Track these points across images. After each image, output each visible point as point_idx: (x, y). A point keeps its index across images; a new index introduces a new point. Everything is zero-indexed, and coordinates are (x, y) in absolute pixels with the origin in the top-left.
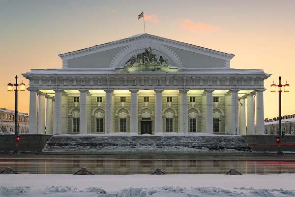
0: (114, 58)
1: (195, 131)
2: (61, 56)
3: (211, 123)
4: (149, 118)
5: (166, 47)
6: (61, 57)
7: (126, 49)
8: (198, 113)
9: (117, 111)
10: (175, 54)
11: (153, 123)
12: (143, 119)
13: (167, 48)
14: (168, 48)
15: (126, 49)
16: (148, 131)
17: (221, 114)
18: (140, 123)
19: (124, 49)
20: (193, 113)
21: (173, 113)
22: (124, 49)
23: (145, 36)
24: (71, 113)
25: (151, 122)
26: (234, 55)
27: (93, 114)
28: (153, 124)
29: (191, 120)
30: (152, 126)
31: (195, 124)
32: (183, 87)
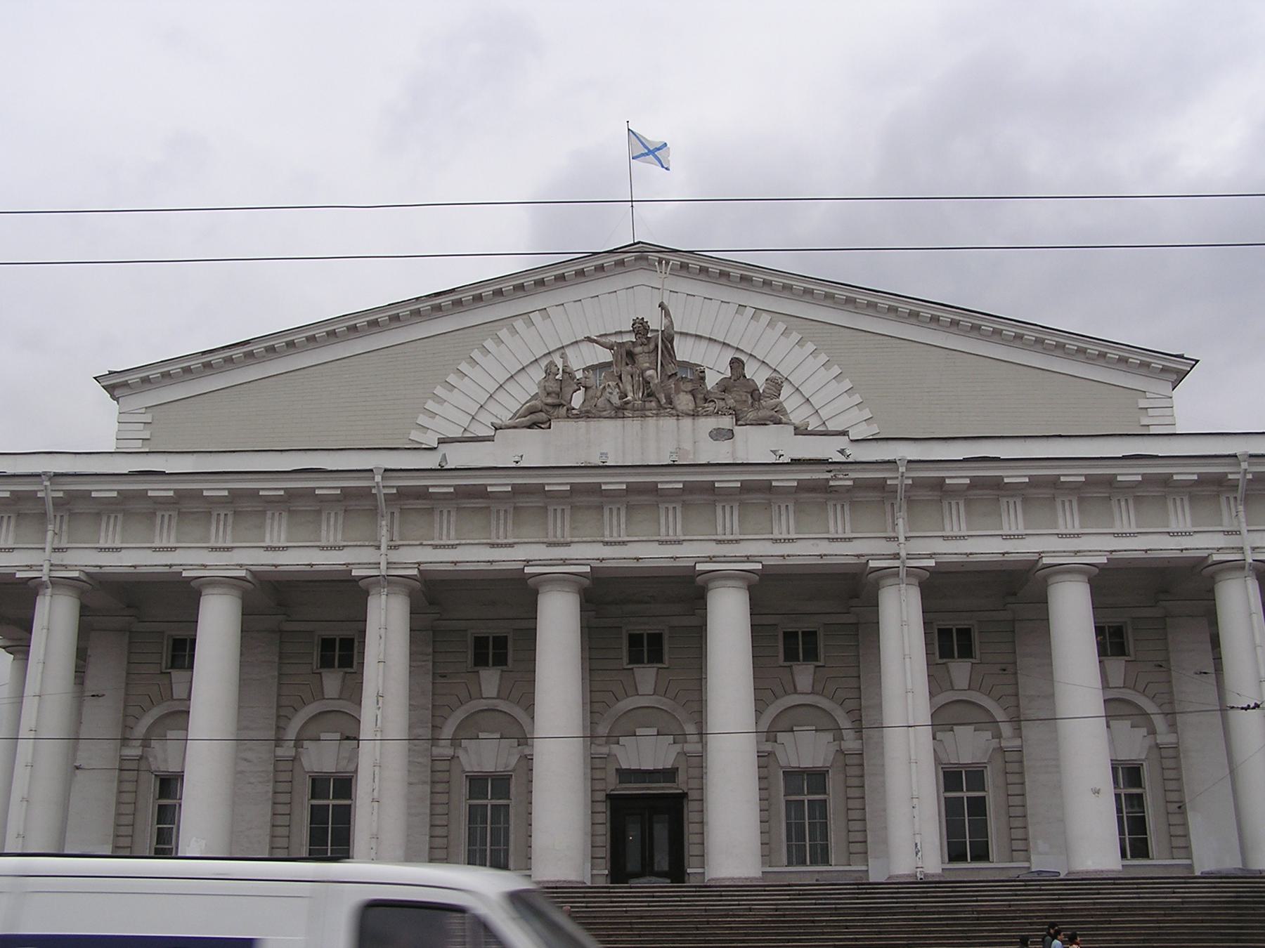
0: (439, 391)
1: (982, 854)
2: (115, 384)
3: (1097, 792)
4: (669, 774)
5: (765, 318)
6: (110, 389)
7: (514, 331)
8: (998, 735)
9: (448, 731)
10: (823, 358)
11: (690, 808)
12: (626, 775)
13: (771, 324)
14: (781, 327)
15: (514, 331)
16: (662, 861)
17: (1152, 732)
18: (601, 807)
19: (504, 334)
20: (964, 733)
21: (829, 737)
22: (504, 334)
23: (641, 256)
24: (146, 742)
25: (684, 796)
26: (1197, 361)
27: (287, 750)
28: (690, 816)
29: (951, 778)
30: (690, 829)
31: (978, 806)
32: (890, 548)
